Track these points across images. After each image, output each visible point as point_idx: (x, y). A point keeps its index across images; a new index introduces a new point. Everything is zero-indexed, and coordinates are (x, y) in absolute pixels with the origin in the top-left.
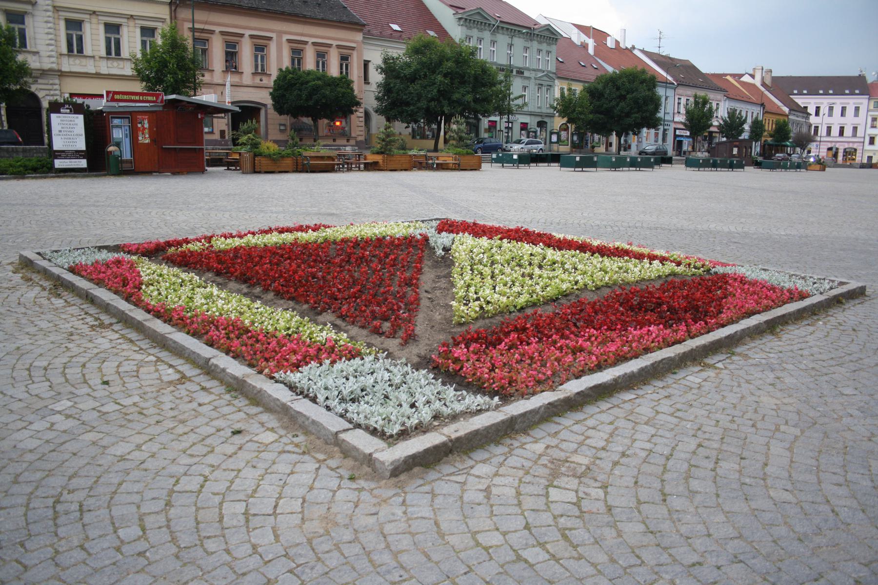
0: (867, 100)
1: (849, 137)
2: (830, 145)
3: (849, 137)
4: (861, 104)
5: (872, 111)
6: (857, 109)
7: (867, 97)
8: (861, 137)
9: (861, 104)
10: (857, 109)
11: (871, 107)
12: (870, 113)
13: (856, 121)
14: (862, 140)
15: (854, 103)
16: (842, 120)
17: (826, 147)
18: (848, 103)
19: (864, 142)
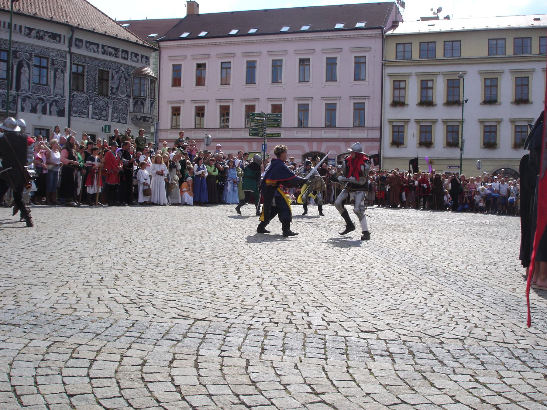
0: (379, 41)
1: (347, 128)
2: (307, 148)
3: (347, 128)
4: (369, 49)
5: (391, 64)
6: (359, 63)
7: (379, 32)
8: (373, 128)
9: (369, 49)
10: (359, 63)
11: (391, 55)
12: (388, 71)
13: (360, 89)
14: (376, 134)
15: (352, 50)
16: (331, 89)
17: (300, 153)
18: (340, 50)
19: (380, 140)
